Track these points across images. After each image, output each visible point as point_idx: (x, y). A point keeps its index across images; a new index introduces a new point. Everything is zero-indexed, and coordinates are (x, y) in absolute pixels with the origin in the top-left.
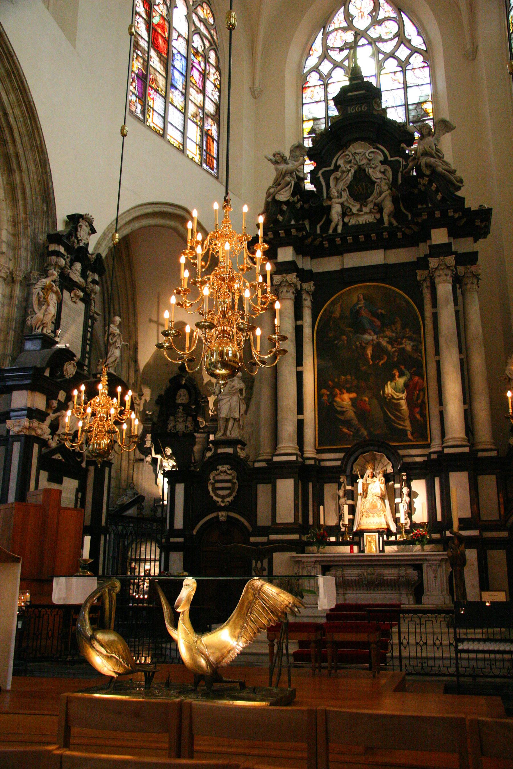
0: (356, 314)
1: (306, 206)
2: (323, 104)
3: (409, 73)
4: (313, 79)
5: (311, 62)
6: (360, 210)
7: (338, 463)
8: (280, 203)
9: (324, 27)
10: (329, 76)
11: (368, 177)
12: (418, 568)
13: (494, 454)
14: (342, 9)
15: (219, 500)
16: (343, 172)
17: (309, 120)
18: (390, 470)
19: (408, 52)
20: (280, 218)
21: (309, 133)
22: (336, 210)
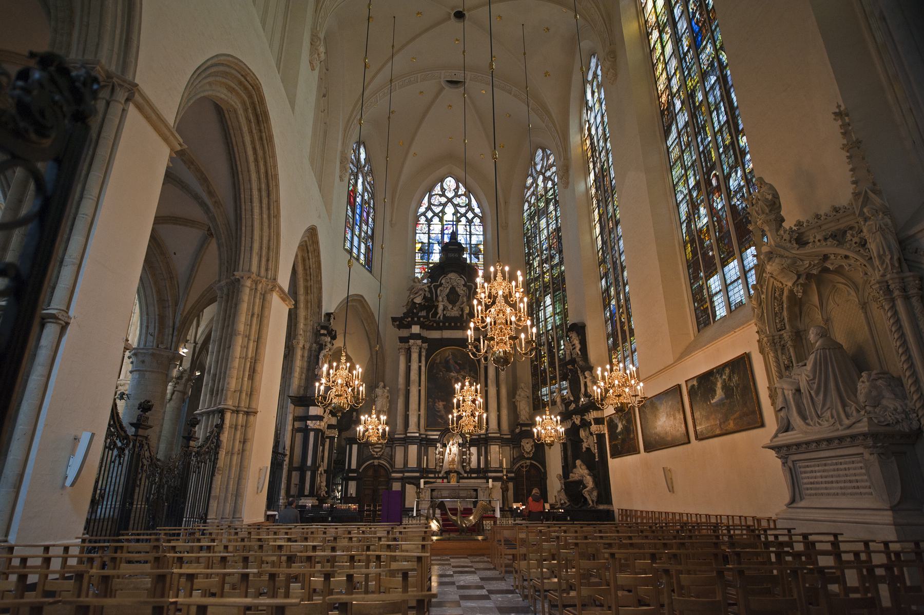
0: (447, 362)
1: (426, 304)
2: (427, 235)
3: (473, 227)
4: (422, 220)
5: (422, 210)
6: (452, 309)
7: (437, 437)
8: (416, 303)
9: (430, 192)
10: (431, 220)
11: (456, 292)
12: (476, 490)
13: (509, 436)
14: (440, 184)
15: (375, 453)
16: (444, 287)
17: (419, 243)
18: (461, 441)
19: (473, 215)
20: (415, 311)
21: (419, 250)
22: (441, 307)
